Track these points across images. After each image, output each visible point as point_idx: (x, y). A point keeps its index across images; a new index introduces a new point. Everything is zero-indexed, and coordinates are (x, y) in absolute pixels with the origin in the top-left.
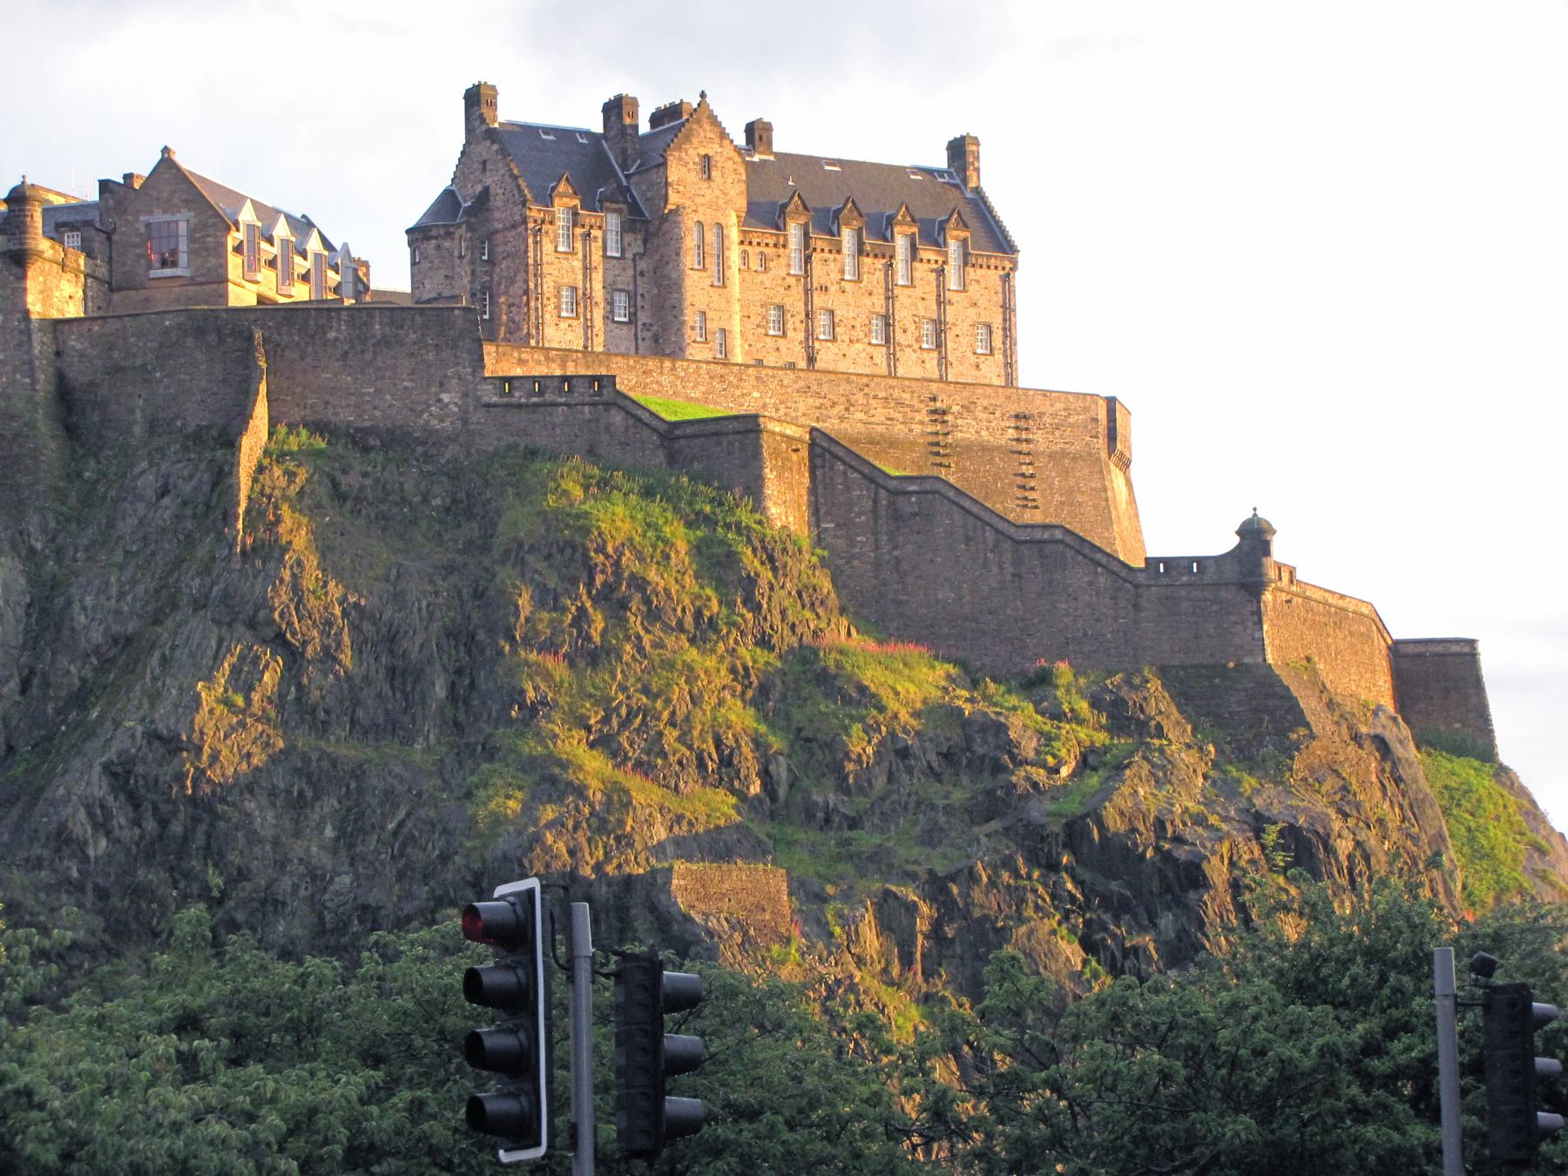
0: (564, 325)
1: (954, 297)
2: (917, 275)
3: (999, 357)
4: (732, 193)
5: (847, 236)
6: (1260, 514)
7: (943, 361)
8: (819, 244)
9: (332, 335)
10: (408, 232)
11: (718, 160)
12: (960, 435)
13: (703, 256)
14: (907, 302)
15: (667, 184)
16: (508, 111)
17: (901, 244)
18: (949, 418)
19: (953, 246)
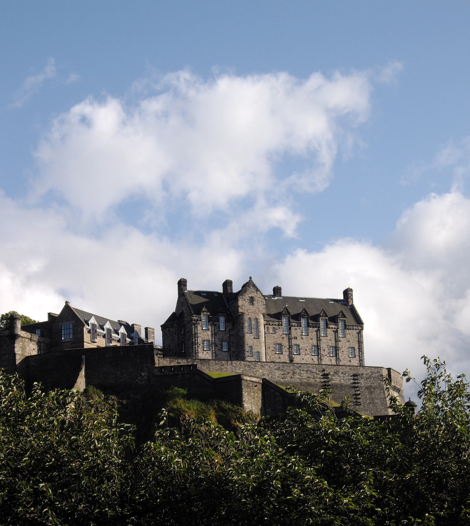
0: (205, 353)
1: (341, 339)
2: (328, 332)
3: (357, 358)
4: (261, 308)
5: (303, 321)
6: (412, 400)
7: (337, 359)
8: (294, 324)
9: (107, 356)
10: (161, 326)
11: (256, 298)
12: (334, 382)
13: (250, 328)
14: (325, 341)
15: (238, 306)
16: (191, 287)
17: (322, 323)
18: (330, 376)
19: (341, 324)
